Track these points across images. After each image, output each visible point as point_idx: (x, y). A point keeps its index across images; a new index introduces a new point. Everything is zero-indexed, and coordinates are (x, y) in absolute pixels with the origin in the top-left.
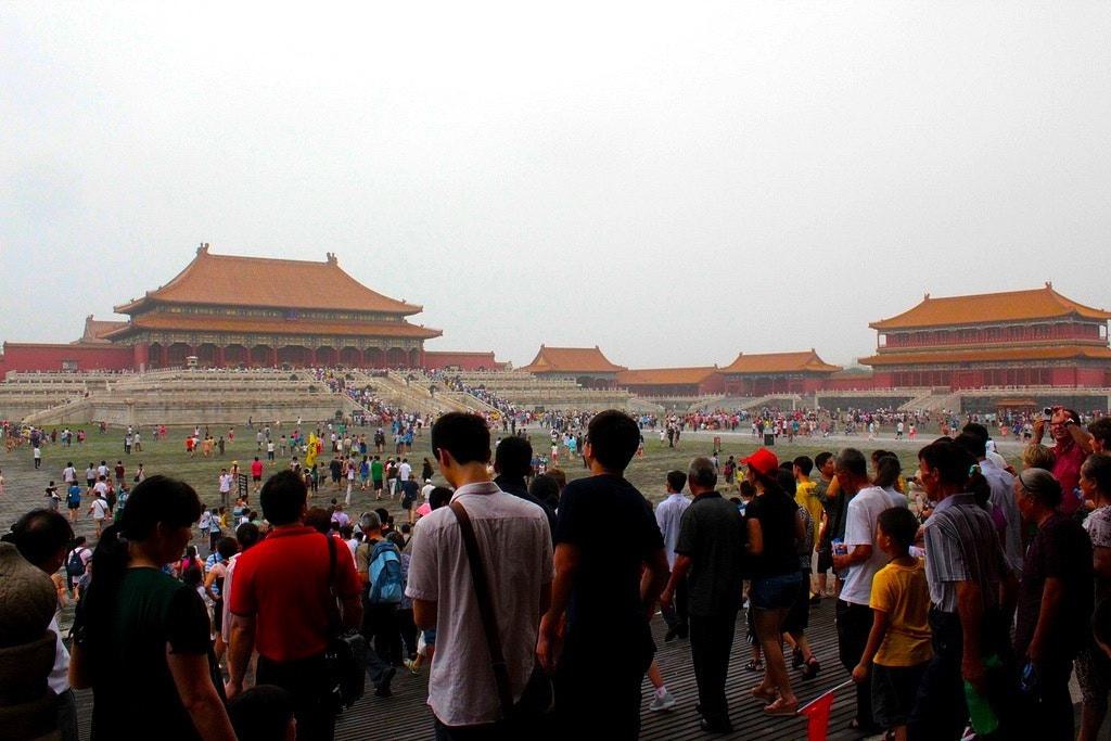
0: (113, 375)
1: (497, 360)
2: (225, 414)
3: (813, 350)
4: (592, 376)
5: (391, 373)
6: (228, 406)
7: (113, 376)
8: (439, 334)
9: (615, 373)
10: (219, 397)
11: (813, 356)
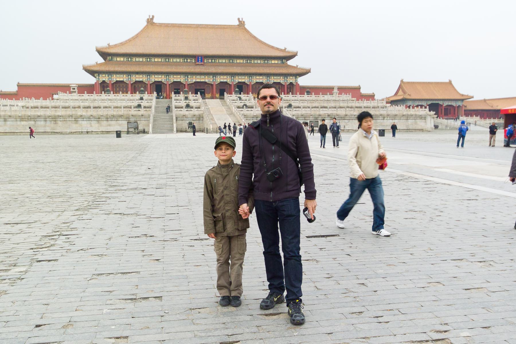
1: (363, 91)
2: (52, 125)
4: (441, 103)
6: (55, 119)
9: (462, 100)
10: (49, 112)
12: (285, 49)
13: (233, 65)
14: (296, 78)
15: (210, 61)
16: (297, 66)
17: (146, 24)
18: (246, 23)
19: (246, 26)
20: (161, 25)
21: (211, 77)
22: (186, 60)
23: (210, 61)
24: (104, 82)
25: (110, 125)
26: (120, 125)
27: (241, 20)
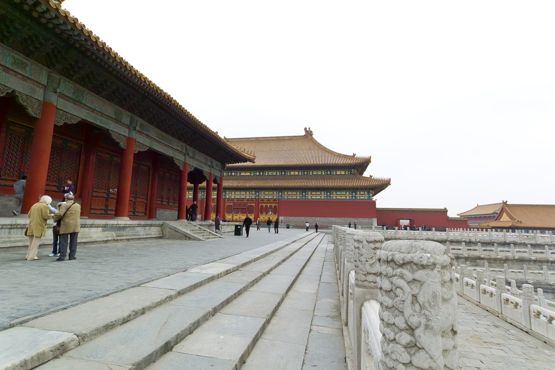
12: (354, 155)
13: (285, 178)
14: (369, 193)
15: (258, 174)
16: (371, 176)
18: (314, 132)
19: (313, 136)
21: (254, 193)
22: (230, 174)
23: (258, 174)
27: (308, 130)
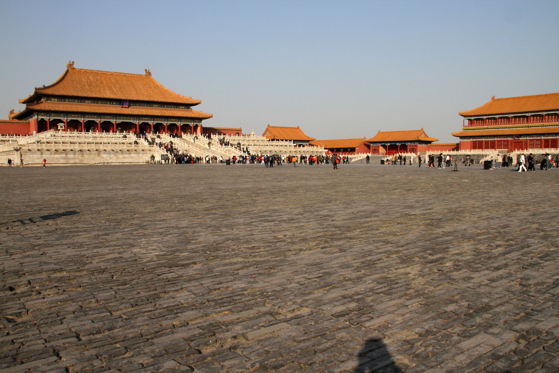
0: (14, 137)
3: (422, 129)
5: (184, 136)
7: (14, 138)
8: (212, 117)
11: (422, 132)
17: (66, 69)
20: (80, 71)
24: (42, 119)
25: (124, 158)
26: (132, 158)
